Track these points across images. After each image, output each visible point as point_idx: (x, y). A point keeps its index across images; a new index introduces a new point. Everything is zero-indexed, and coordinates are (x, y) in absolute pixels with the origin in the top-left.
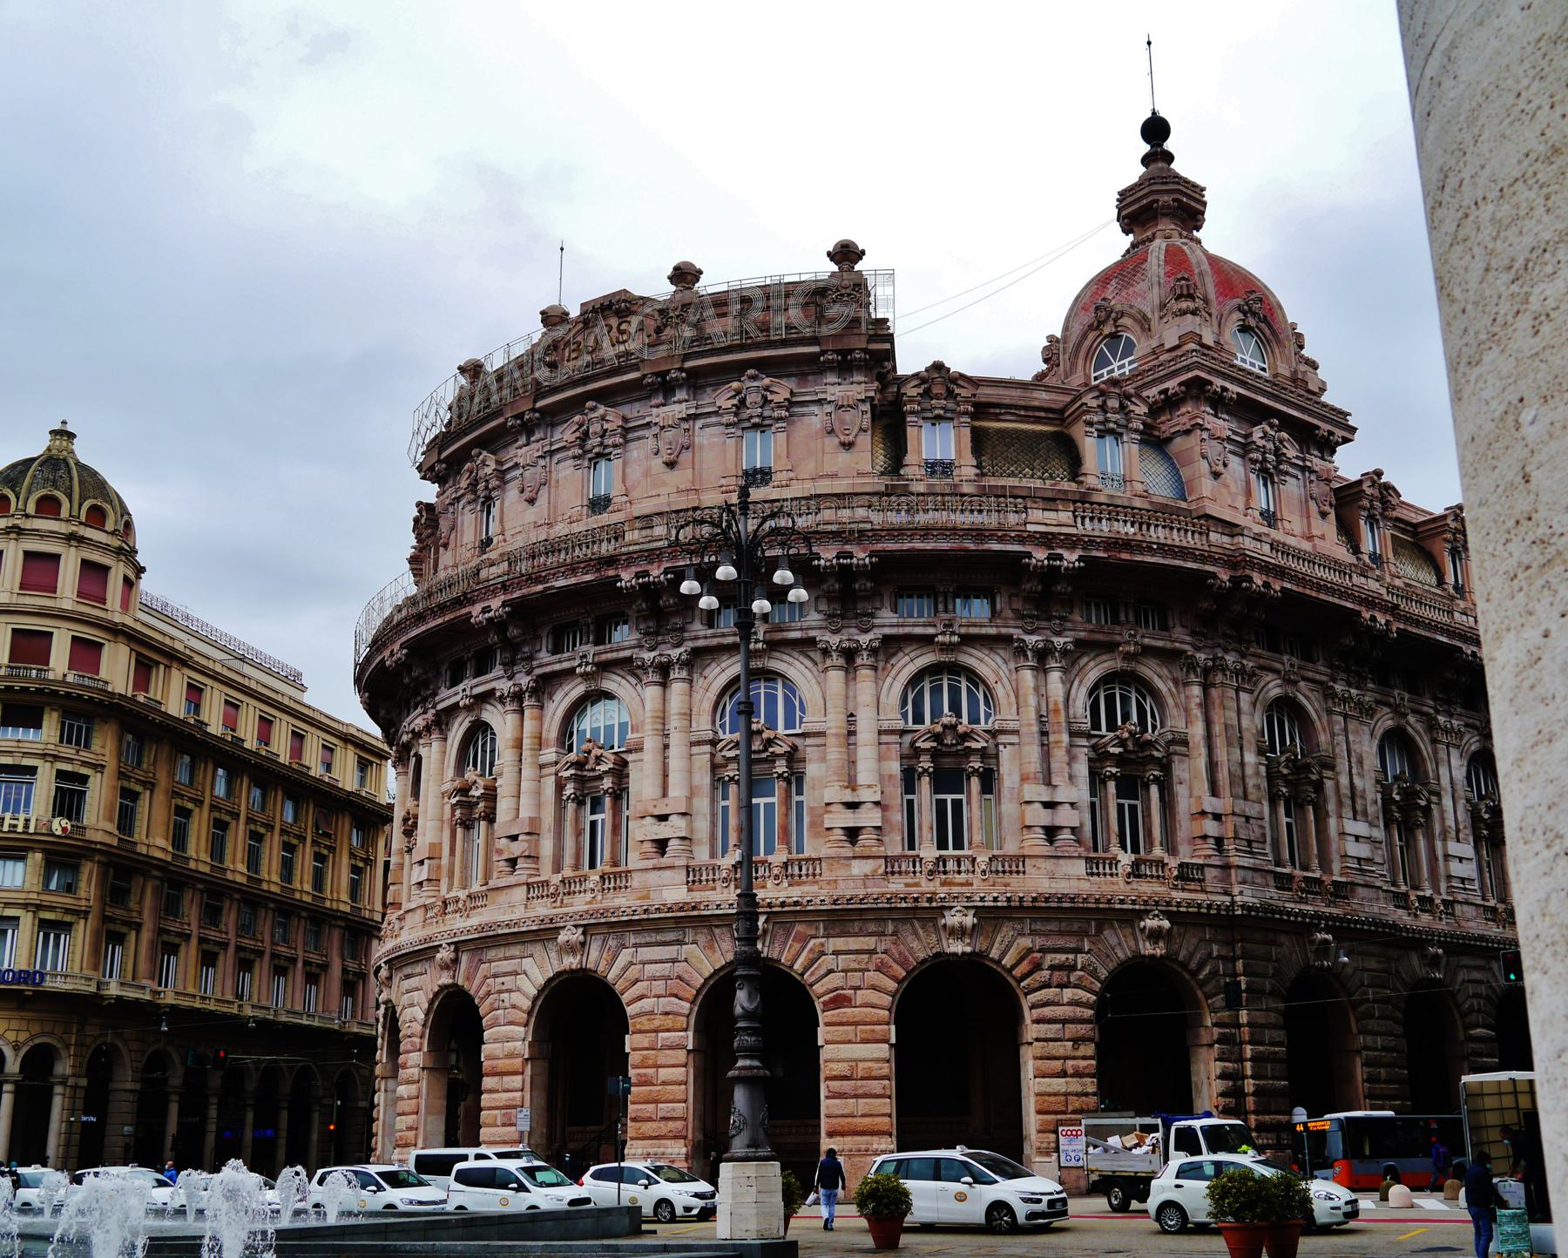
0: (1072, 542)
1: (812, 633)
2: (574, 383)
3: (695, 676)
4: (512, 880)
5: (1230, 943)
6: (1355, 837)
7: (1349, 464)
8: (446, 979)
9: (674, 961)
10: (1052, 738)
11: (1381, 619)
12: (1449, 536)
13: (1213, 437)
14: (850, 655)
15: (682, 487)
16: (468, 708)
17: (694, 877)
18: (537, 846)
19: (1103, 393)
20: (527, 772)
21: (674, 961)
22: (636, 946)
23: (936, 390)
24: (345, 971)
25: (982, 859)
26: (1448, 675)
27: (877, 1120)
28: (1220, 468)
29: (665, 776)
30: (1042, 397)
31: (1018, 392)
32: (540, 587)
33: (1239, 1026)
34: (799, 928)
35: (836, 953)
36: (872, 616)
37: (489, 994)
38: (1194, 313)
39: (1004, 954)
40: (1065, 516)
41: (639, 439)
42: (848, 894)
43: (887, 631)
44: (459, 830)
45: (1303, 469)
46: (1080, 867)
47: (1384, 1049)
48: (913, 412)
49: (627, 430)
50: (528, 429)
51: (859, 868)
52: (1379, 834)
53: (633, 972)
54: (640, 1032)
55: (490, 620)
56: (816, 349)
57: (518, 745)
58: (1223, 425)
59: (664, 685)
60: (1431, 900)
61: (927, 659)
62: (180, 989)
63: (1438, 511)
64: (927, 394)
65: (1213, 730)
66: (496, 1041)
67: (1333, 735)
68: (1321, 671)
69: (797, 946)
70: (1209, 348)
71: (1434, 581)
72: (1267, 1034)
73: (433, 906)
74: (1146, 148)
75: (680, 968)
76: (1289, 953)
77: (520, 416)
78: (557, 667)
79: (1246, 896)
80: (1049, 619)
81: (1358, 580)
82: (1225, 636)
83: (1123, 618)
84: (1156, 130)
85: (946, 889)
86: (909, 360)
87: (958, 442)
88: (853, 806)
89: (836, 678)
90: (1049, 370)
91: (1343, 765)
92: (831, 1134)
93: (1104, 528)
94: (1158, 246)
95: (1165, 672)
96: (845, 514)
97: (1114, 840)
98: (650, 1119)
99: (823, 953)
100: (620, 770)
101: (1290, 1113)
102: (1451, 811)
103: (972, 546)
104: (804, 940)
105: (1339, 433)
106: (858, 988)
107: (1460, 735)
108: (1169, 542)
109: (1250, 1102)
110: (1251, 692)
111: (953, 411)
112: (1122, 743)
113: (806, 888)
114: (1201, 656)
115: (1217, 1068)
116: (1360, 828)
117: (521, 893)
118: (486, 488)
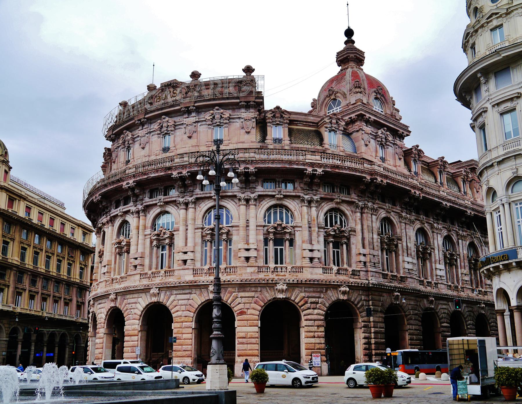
0: (320, 166)
1: (235, 194)
2: (158, 110)
3: (197, 207)
4: (135, 272)
5: (368, 296)
6: (407, 262)
7: (408, 143)
8: (113, 305)
9: (188, 299)
10: (312, 229)
11: (418, 193)
12: (439, 167)
13: (366, 133)
14: (247, 201)
15: (194, 145)
16: (121, 216)
17: (195, 272)
18: (143, 262)
19: (331, 118)
20: (141, 237)
21: (188, 299)
22: (176, 294)
23: (277, 115)
24: (77, 302)
25: (289, 268)
26: (438, 211)
27: (254, 351)
28: (368, 143)
29: (186, 239)
30: (311, 119)
31: (304, 117)
32: (146, 177)
33: (370, 322)
34: (229, 289)
35: (241, 297)
36: (255, 188)
37: (127, 310)
38: (360, 93)
39: (296, 298)
40: (318, 157)
41: (179, 128)
42: (246, 278)
43: (260, 193)
44: (118, 256)
45: (394, 144)
46: (321, 271)
47: (415, 330)
48: (269, 122)
49: (176, 126)
50: (142, 124)
51: (249, 270)
52: (415, 261)
53: (175, 303)
54: (177, 322)
55: (129, 187)
56: (238, 101)
57: (138, 228)
58: (369, 129)
59: (186, 209)
60: (431, 283)
61: (273, 202)
62: (22, 307)
63: (436, 158)
64: (274, 116)
65: (363, 226)
66: (129, 325)
67: (401, 230)
68: (398, 209)
69: (229, 295)
70: (365, 104)
71: (434, 181)
72: (379, 325)
73: (109, 281)
74: (346, 39)
75: (190, 302)
76: (386, 299)
77: (140, 120)
78: (151, 203)
79: (373, 280)
80: (312, 190)
81: (410, 180)
82: (368, 197)
83: (336, 190)
84: (349, 33)
85: (277, 277)
86: (269, 105)
87: (284, 133)
88: (248, 250)
89: (243, 208)
90: (313, 110)
91: (404, 239)
92: (239, 356)
93: (331, 162)
94: (349, 71)
95: (349, 208)
96: (247, 155)
97: (332, 262)
98: (180, 351)
99: (237, 297)
100: (172, 237)
101: (385, 350)
102: (438, 254)
103: (288, 166)
104: (231, 293)
105: (406, 133)
106: (249, 309)
107: (441, 230)
108: (351, 166)
109: (373, 346)
110: (376, 215)
111: (283, 122)
112: (335, 231)
113: (232, 276)
114: (360, 203)
115: (363, 335)
116: (409, 259)
118: (128, 143)
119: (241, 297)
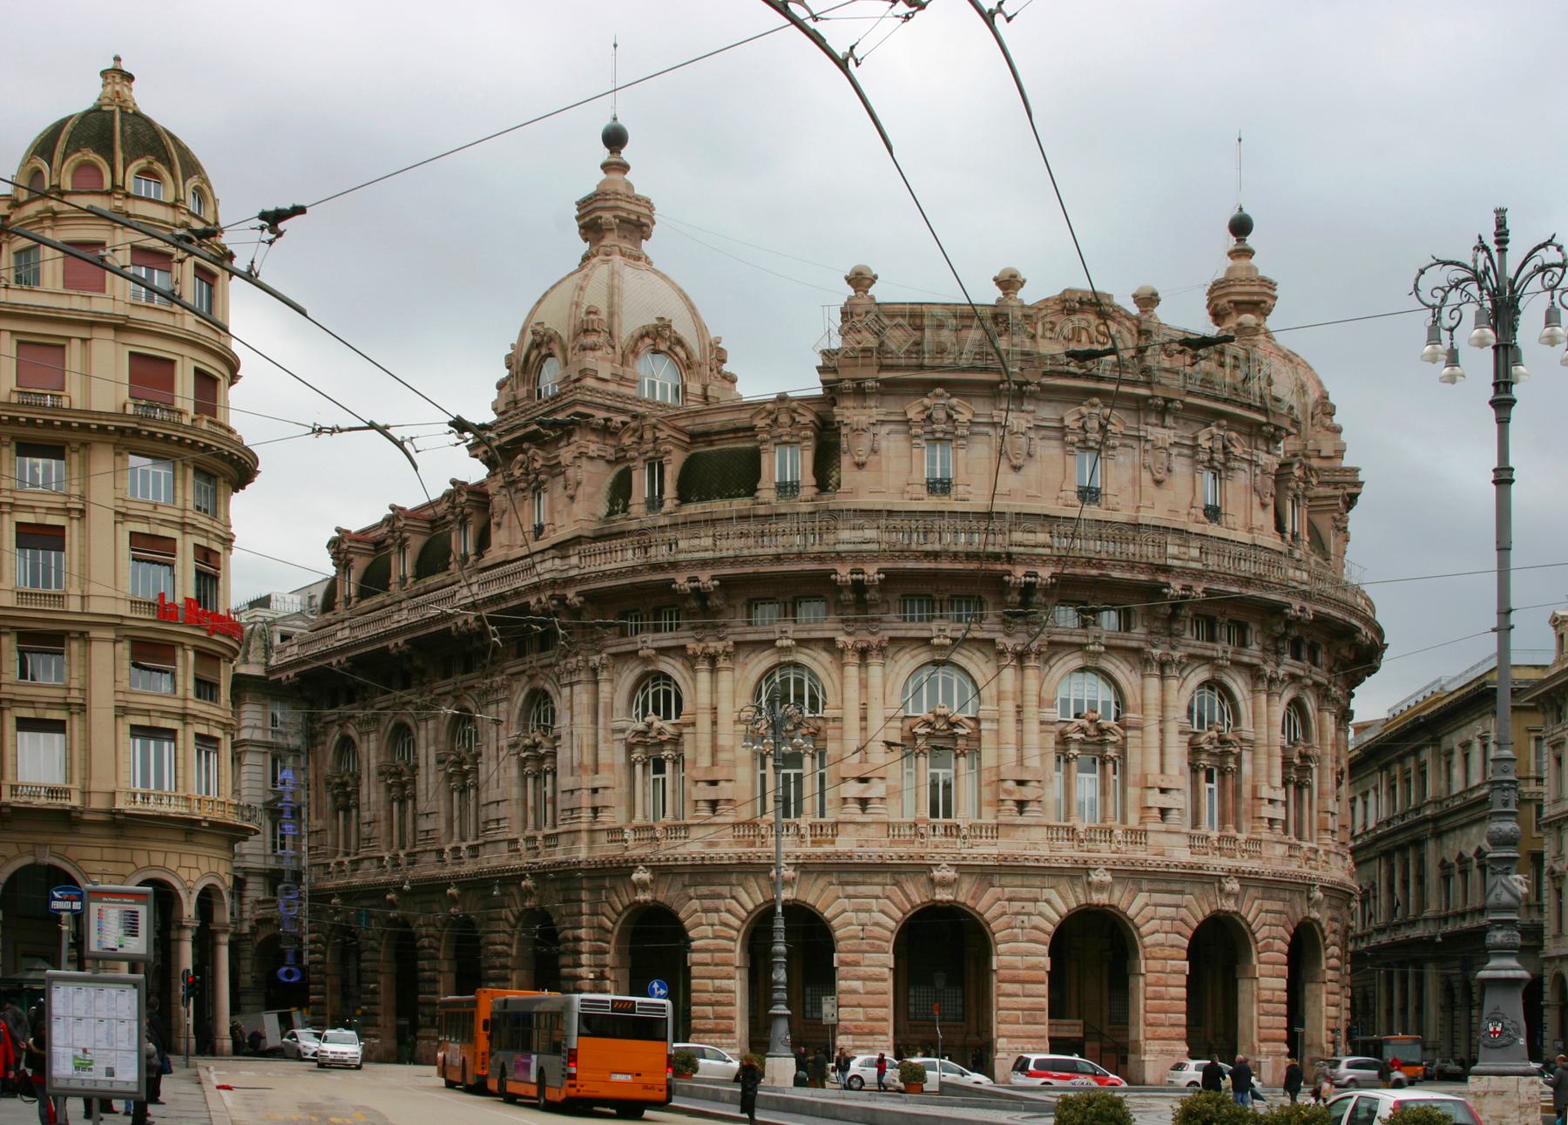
1: (1255, 661)
8: (943, 895)
9: (1178, 906)
16: (942, 647)
17: (1196, 842)
20: (1032, 726)
21: (1178, 906)
22: (1150, 891)
34: (1251, 891)
35: (1267, 911)
42: (1281, 868)
51: (1281, 850)
53: (1149, 911)
59: (1163, 677)
66: (1013, 954)
75: (1183, 912)
78: (1066, 639)
89: (1264, 697)
117: (1040, 834)
119: (1267, 911)
